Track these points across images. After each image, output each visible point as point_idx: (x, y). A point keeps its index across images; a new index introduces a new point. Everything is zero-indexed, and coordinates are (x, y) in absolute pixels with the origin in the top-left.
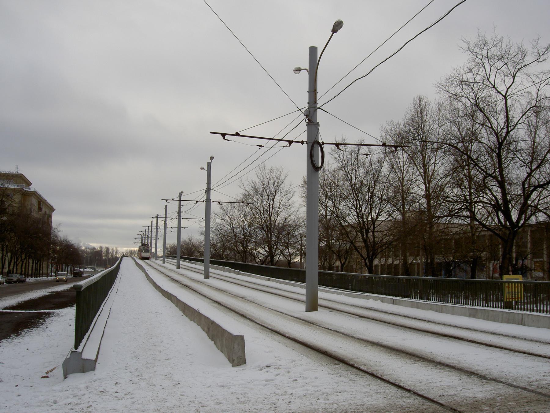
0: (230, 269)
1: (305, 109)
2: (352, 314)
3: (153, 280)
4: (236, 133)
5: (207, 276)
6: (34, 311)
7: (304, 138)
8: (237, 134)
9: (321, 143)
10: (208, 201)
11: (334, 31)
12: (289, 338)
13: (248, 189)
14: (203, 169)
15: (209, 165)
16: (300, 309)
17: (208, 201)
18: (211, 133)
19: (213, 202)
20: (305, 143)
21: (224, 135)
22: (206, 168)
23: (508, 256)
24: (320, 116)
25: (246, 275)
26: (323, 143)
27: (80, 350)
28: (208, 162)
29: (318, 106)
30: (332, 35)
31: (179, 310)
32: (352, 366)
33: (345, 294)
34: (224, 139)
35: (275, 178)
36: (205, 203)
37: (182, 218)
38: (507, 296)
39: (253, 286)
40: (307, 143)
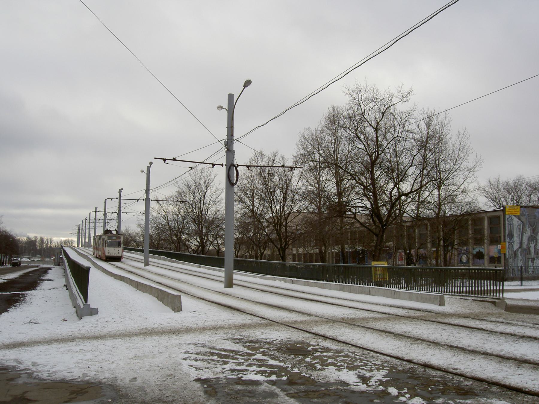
0: (166, 257)
1: (225, 140)
3: (102, 267)
4: (174, 158)
5: (147, 264)
6: (8, 293)
7: (224, 161)
8: (175, 159)
9: (236, 166)
10: (147, 200)
11: (245, 86)
12: (209, 301)
13: (181, 187)
14: (142, 171)
15: (149, 169)
16: (221, 287)
17: (147, 200)
18: (155, 158)
19: (152, 200)
20: (224, 165)
21: (165, 160)
22: (146, 171)
23: (379, 247)
24: (236, 146)
25: (180, 263)
26: (238, 165)
27: (88, 303)
28: (147, 167)
29: (235, 138)
30: (244, 89)
31: (132, 287)
32: (243, 312)
33: (259, 277)
34: (165, 163)
35: (206, 177)
36: (145, 201)
37: (122, 212)
38: (374, 277)
39: (187, 272)
40: (226, 166)
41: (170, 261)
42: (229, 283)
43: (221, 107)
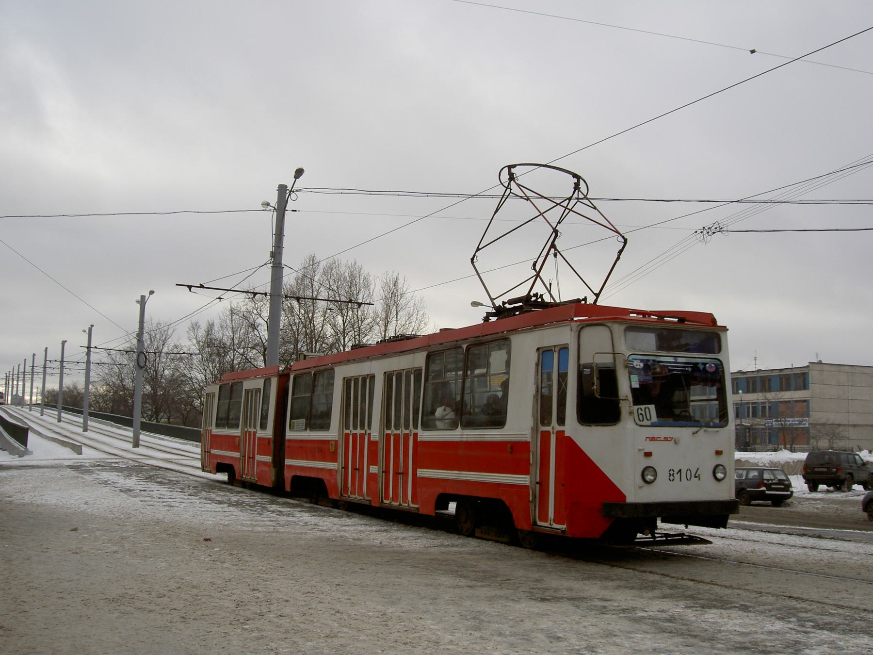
0: (113, 423)
2: (116, 438)
5: (85, 430)
14: (84, 331)
15: (90, 330)
22: (87, 332)
25: (125, 430)
41: (116, 427)
42: (136, 444)
43: (139, 302)
